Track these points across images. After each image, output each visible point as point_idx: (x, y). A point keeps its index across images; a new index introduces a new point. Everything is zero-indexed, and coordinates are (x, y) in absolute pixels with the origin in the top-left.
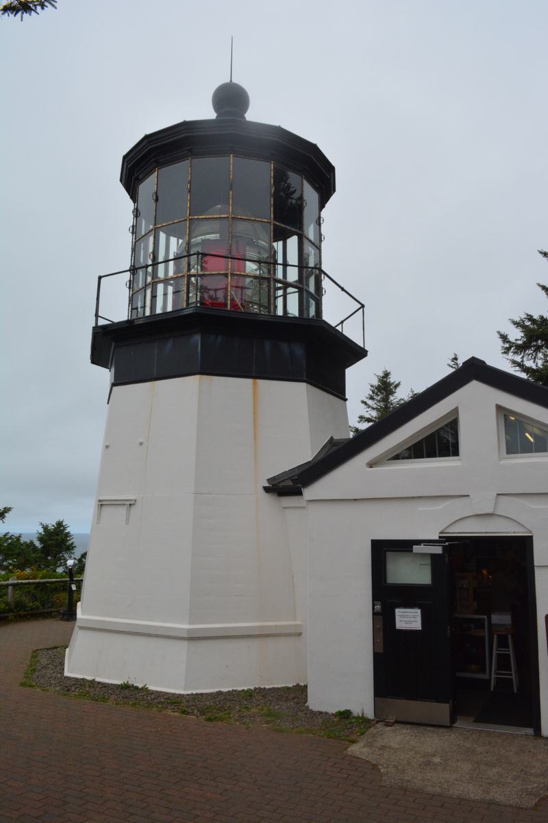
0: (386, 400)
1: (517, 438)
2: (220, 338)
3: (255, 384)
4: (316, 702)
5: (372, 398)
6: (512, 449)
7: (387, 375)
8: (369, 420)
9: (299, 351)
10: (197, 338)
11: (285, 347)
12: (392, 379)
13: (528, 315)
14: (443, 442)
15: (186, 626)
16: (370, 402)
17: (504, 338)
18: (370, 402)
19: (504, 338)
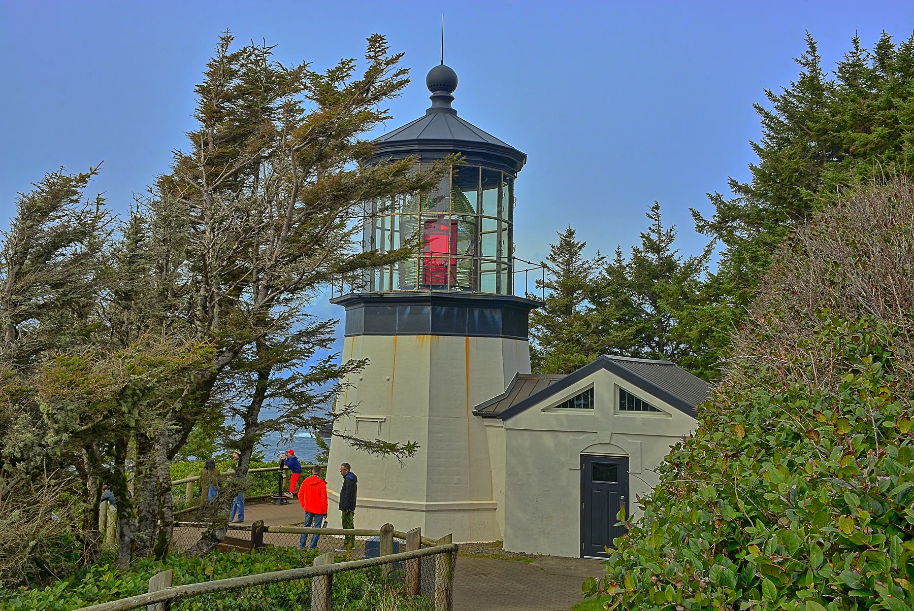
0: (568, 263)
1: (628, 402)
2: (444, 309)
3: (467, 341)
4: (506, 548)
5: (553, 259)
6: (622, 407)
7: (571, 234)
8: (549, 286)
9: (498, 315)
10: (428, 309)
11: (488, 312)
12: (576, 239)
13: (732, 181)
14: (585, 399)
15: (425, 503)
16: (550, 264)
17: (696, 215)
18: (550, 264)
19: (696, 215)
